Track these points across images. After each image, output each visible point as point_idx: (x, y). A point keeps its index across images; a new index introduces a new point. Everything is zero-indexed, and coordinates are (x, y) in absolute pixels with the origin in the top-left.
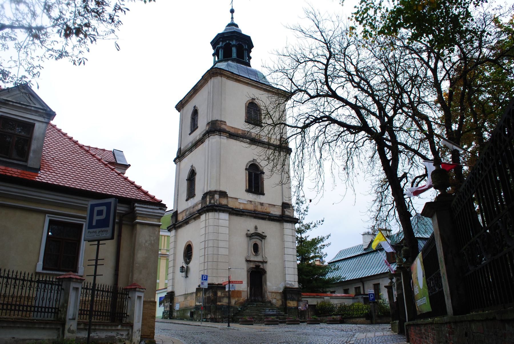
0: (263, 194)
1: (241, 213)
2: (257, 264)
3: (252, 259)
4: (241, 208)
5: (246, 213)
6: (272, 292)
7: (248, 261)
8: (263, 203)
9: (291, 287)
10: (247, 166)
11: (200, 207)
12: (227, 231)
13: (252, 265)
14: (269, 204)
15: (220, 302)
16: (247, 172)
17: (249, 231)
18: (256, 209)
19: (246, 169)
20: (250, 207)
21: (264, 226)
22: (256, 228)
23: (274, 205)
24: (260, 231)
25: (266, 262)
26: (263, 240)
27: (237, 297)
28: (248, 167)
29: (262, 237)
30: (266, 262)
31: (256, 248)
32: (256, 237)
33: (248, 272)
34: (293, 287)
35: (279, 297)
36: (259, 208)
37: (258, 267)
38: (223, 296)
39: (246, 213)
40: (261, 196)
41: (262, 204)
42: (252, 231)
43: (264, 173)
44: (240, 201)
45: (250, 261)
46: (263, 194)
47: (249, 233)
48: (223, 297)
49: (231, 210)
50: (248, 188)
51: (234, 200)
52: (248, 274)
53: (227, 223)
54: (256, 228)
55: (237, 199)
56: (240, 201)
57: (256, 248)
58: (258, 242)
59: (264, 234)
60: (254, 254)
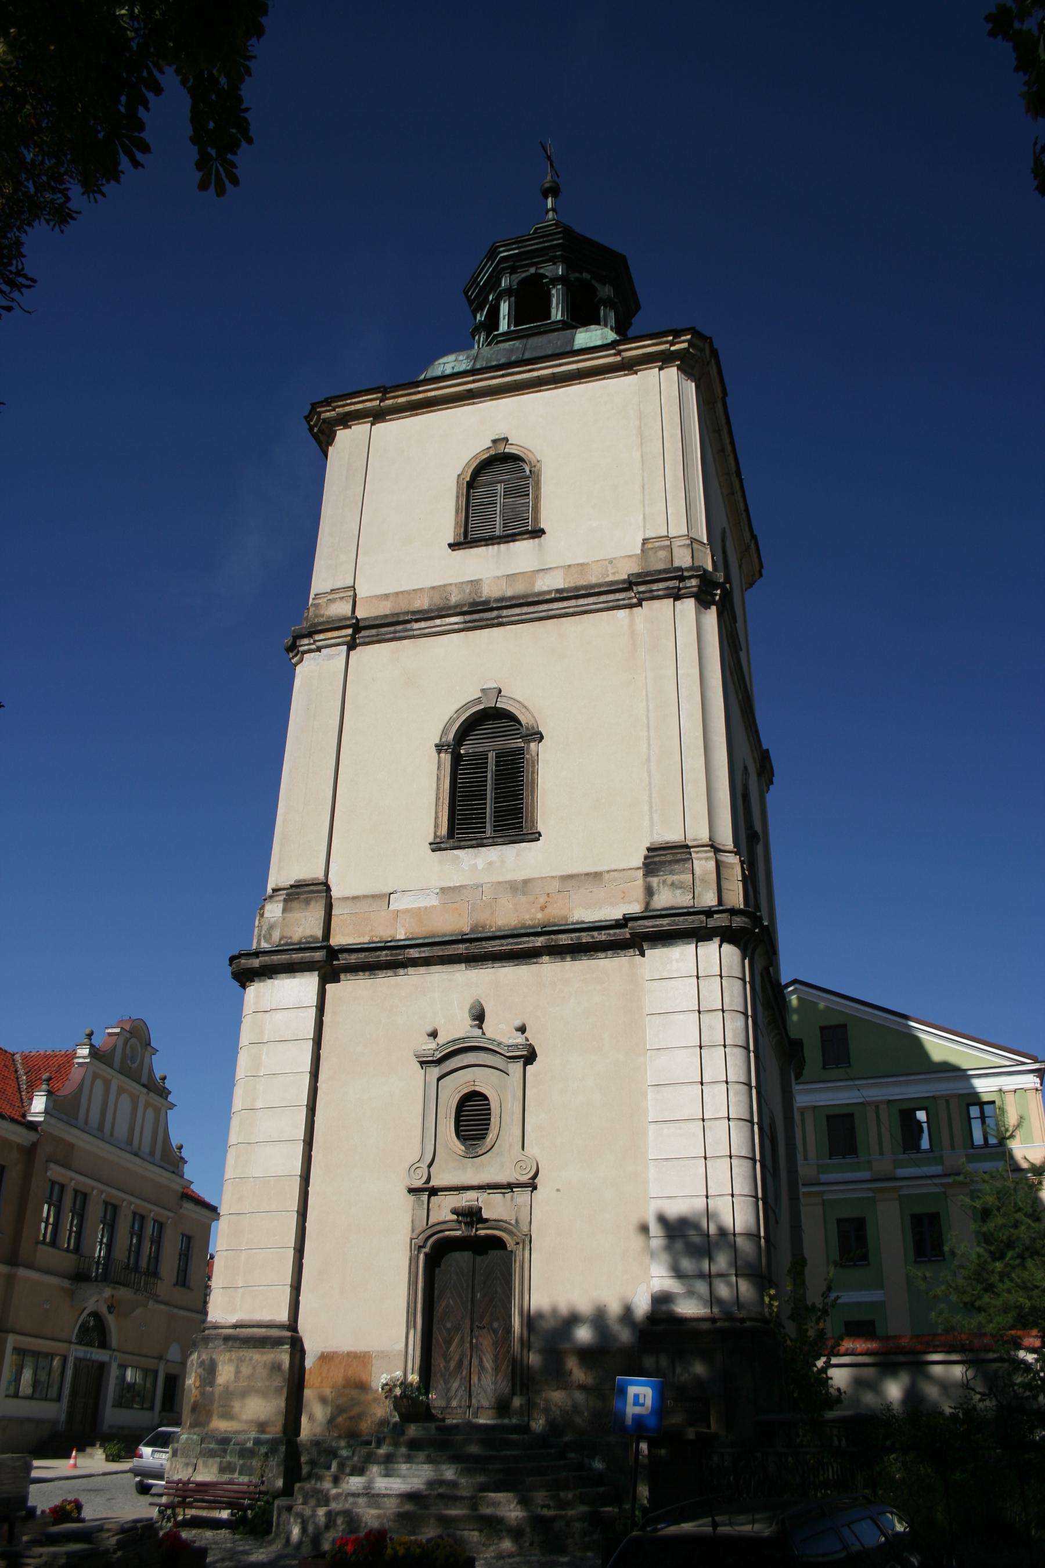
0: (536, 837)
1: (384, 956)
4: (401, 935)
5: (414, 953)
8: (526, 882)
10: (445, 731)
15: (227, 1415)
16: (446, 758)
19: (440, 748)
20: (453, 922)
23: (597, 876)
31: (473, 1119)
36: (507, 915)
41: (521, 887)
46: (536, 837)
48: (244, 1394)
50: (444, 831)
52: (413, 1261)
56: (398, 903)
57: (473, 1119)
60: (458, 1146)
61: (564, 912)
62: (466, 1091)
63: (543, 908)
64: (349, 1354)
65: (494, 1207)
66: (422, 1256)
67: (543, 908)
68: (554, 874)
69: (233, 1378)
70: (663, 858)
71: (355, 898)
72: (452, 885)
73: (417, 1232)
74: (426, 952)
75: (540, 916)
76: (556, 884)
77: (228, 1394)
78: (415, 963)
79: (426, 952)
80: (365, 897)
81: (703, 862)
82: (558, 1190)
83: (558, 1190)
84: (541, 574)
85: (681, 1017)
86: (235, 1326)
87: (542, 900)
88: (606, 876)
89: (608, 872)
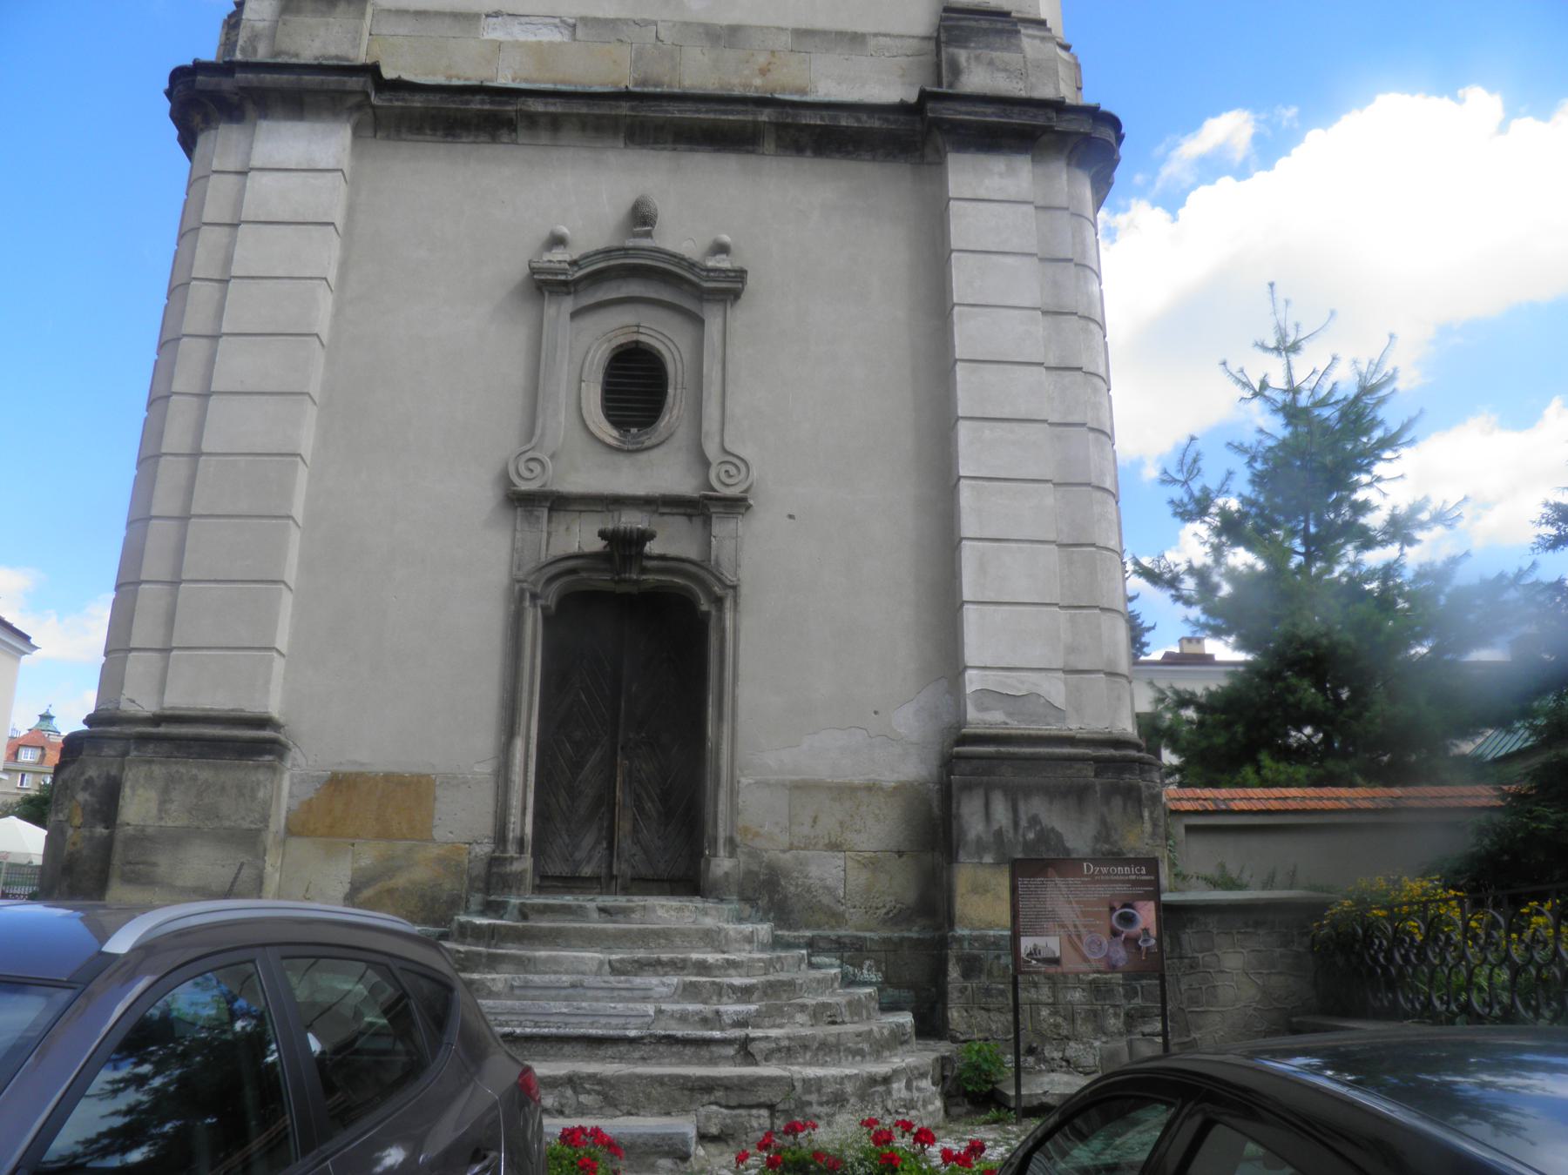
2: (632, 520)
5: (537, 106)
6: (801, 788)
7: (525, 502)
8: (734, 30)
9: (1017, 726)
12: (325, 253)
13: (583, 536)
17: (558, 241)
23: (855, 40)
24: (680, 236)
25: (737, 505)
27: (385, 835)
30: (737, 505)
31: (635, 389)
32: (634, 288)
33: (519, 597)
34: (1053, 728)
35: (877, 830)
38: (176, 818)
39: (537, 106)
44: (494, 32)
45: (558, 503)
48: (177, 839)
49: (354, 83)
53: (330, 197)
54: (641, 217)
55: (475, 17)
58: (664, 334)
59: (722, 262)
60: (609, 433)
62: (622, 340)
64: (388, 777)
65: (671, 540)
67: (763, 72)
68: (783, 25)
69: (154, 811)
70: (973, 24)
71: (420, 14)
72: (600, 15)
73: (530, 565)
74: (556, 107)
75: (758, 82)
76: (786, 40)
77: (142, 838)
78: (532, 121)
79: (556, 107)
81: (1037, 42)
82: (791, 517)
83: (791, 517)
85: (1009, 260)
86: (157, 720)
87: (762, 59)
88: (872, 42)
89: (876, 35)
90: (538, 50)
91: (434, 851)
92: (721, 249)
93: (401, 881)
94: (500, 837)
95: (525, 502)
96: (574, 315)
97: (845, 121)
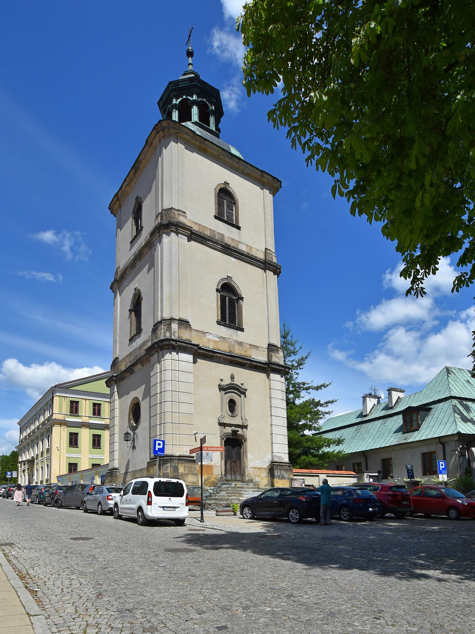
3: (228, 420)
7: (222, 425)
8: (241, 342)
10: (218, 285)
11: (149, 344)
12: (190, 378)
13: (229, 430)
14: (250, 345)
17: (222, 380)
18: (232, 349)
20: (224, 348)
21: (243, 376)
22: (232, 378)
23: (257, 347)
24: (237, 382)
26: (243, 396)
28: (219, 287)
29: (242, 392)
30: (246, 427)
36: (238, 351)
37: (235, 432)
40: (239, 332)
41: (241, 344)
42: (227, 381)
43: (242, 299)
47: (222, 383)
49: (196, 348)
50: (220, 318)
51: (200, 334)
54: (232, 378)
56: (208, 336)
58: (235, 397)
59: (243, 387)
60: (230, 414)
61: (250, 355)
63: (246, 352)
66: (223, 441)
67: (246, 352)
71: (197, 330)
76: (248, 346)
80: (200, 331)
84: (240, 243)
90: (215, 342)
91: (214, 476)
92: (242, 384)
93: (210, 481)
94: (222, 475)
95: (222, 425)
96: (225, 394)
97: (258, 364)
